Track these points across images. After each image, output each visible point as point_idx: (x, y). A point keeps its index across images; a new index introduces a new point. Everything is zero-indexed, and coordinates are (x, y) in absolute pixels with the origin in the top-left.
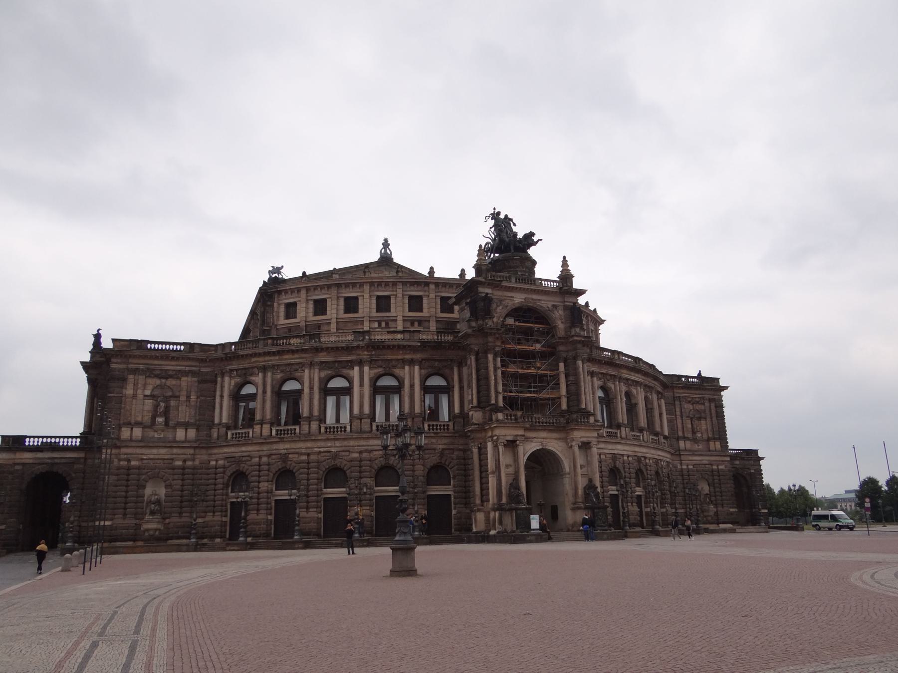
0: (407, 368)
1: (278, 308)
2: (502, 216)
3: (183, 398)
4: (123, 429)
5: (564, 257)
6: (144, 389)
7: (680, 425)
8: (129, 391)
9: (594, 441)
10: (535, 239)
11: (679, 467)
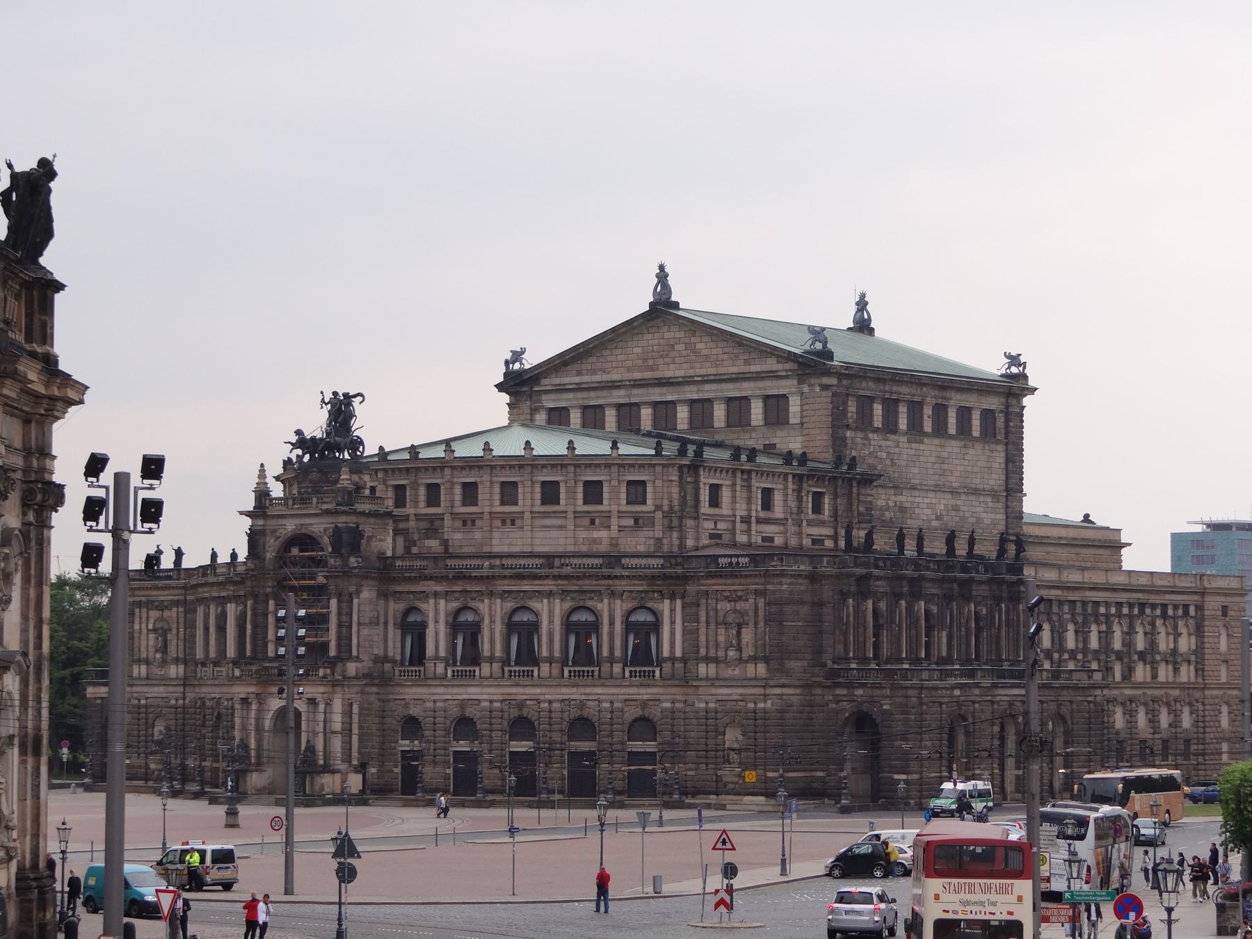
3: (174, 631)
7: (703, 638)
8: (137, 627)
9: (319, 698)
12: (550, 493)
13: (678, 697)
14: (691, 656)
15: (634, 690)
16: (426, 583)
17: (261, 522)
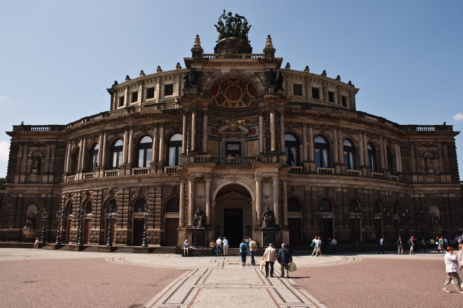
0: (155, 129)
1: (116, 100)
2: (233, 15)
3: (47, 158)
4: (16, 177)
5: (269, 36)
6: (28, 154)
7: (413, 164)
8: (20, 155)
10: (248, 26)
11: (412, 196)
12: (315, 92)
13: (404, 192)
14: (408, 171)
15: (394, 187)
16: (301, 117)
17: (201, 67)
